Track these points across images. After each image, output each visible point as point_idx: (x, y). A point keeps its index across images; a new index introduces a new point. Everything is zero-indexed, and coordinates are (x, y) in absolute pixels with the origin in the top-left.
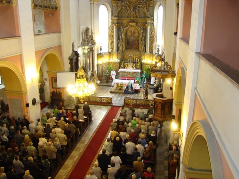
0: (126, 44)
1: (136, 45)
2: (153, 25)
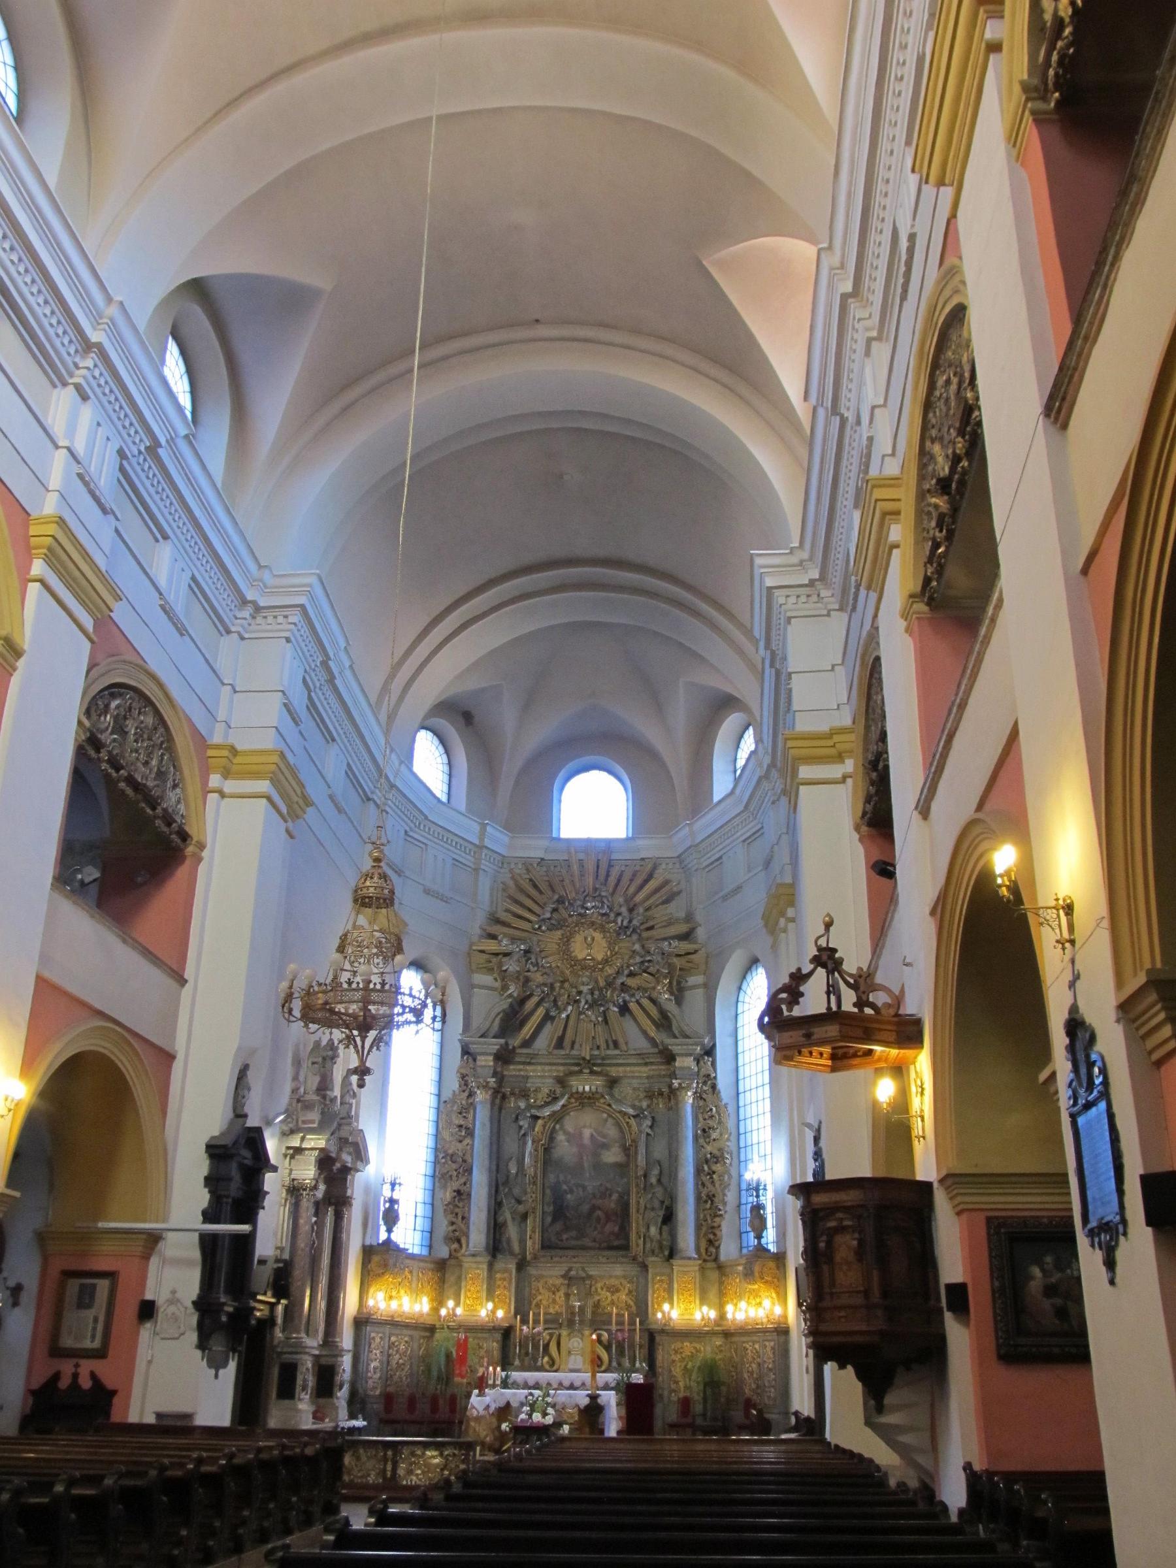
0: (549, 1219)
1: (608, 1219)
2: (714, 1087)
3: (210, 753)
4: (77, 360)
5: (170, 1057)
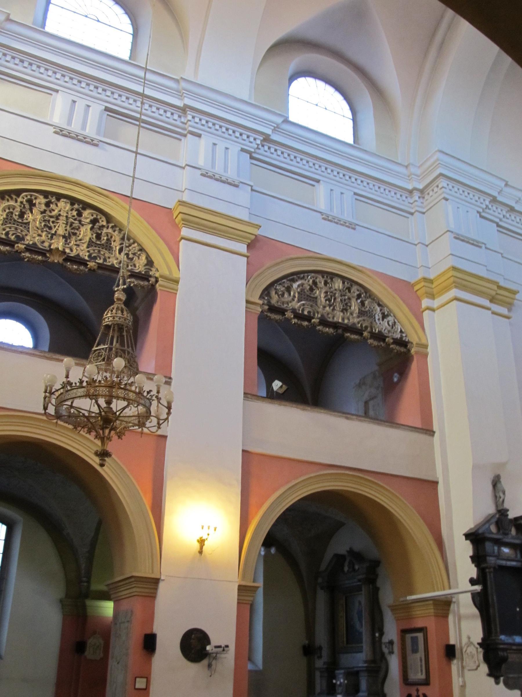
3: (416, 288)
4: (183, 120)
5: (435, 483)
